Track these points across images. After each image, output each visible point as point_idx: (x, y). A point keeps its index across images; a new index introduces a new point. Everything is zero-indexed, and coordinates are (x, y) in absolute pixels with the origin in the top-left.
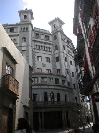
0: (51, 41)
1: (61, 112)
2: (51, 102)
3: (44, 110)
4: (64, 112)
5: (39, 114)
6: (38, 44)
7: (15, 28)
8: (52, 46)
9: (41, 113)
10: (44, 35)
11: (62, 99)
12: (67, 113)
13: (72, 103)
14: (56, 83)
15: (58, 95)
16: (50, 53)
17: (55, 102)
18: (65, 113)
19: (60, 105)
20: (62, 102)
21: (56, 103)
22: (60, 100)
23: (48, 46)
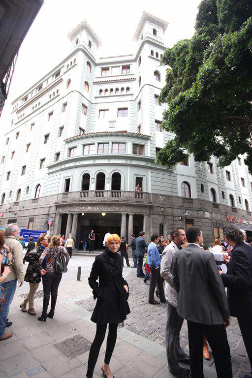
0: (134, 74)
1: (119, 216)
3: (77, 210)
4: (127, 216)
5: (69, 217)
6: (103, 87)
7: (61, 69)
9: (72, 215)
10: (119, 66)
11: (128, 184)
12: (138, 221)
13: (161, 195)
14: (135, 152)
15: (116, 178)
16: (129, 98)
18: (131, 218)
19: (116, 199)
22: (120, 189)
23: (125, 85)
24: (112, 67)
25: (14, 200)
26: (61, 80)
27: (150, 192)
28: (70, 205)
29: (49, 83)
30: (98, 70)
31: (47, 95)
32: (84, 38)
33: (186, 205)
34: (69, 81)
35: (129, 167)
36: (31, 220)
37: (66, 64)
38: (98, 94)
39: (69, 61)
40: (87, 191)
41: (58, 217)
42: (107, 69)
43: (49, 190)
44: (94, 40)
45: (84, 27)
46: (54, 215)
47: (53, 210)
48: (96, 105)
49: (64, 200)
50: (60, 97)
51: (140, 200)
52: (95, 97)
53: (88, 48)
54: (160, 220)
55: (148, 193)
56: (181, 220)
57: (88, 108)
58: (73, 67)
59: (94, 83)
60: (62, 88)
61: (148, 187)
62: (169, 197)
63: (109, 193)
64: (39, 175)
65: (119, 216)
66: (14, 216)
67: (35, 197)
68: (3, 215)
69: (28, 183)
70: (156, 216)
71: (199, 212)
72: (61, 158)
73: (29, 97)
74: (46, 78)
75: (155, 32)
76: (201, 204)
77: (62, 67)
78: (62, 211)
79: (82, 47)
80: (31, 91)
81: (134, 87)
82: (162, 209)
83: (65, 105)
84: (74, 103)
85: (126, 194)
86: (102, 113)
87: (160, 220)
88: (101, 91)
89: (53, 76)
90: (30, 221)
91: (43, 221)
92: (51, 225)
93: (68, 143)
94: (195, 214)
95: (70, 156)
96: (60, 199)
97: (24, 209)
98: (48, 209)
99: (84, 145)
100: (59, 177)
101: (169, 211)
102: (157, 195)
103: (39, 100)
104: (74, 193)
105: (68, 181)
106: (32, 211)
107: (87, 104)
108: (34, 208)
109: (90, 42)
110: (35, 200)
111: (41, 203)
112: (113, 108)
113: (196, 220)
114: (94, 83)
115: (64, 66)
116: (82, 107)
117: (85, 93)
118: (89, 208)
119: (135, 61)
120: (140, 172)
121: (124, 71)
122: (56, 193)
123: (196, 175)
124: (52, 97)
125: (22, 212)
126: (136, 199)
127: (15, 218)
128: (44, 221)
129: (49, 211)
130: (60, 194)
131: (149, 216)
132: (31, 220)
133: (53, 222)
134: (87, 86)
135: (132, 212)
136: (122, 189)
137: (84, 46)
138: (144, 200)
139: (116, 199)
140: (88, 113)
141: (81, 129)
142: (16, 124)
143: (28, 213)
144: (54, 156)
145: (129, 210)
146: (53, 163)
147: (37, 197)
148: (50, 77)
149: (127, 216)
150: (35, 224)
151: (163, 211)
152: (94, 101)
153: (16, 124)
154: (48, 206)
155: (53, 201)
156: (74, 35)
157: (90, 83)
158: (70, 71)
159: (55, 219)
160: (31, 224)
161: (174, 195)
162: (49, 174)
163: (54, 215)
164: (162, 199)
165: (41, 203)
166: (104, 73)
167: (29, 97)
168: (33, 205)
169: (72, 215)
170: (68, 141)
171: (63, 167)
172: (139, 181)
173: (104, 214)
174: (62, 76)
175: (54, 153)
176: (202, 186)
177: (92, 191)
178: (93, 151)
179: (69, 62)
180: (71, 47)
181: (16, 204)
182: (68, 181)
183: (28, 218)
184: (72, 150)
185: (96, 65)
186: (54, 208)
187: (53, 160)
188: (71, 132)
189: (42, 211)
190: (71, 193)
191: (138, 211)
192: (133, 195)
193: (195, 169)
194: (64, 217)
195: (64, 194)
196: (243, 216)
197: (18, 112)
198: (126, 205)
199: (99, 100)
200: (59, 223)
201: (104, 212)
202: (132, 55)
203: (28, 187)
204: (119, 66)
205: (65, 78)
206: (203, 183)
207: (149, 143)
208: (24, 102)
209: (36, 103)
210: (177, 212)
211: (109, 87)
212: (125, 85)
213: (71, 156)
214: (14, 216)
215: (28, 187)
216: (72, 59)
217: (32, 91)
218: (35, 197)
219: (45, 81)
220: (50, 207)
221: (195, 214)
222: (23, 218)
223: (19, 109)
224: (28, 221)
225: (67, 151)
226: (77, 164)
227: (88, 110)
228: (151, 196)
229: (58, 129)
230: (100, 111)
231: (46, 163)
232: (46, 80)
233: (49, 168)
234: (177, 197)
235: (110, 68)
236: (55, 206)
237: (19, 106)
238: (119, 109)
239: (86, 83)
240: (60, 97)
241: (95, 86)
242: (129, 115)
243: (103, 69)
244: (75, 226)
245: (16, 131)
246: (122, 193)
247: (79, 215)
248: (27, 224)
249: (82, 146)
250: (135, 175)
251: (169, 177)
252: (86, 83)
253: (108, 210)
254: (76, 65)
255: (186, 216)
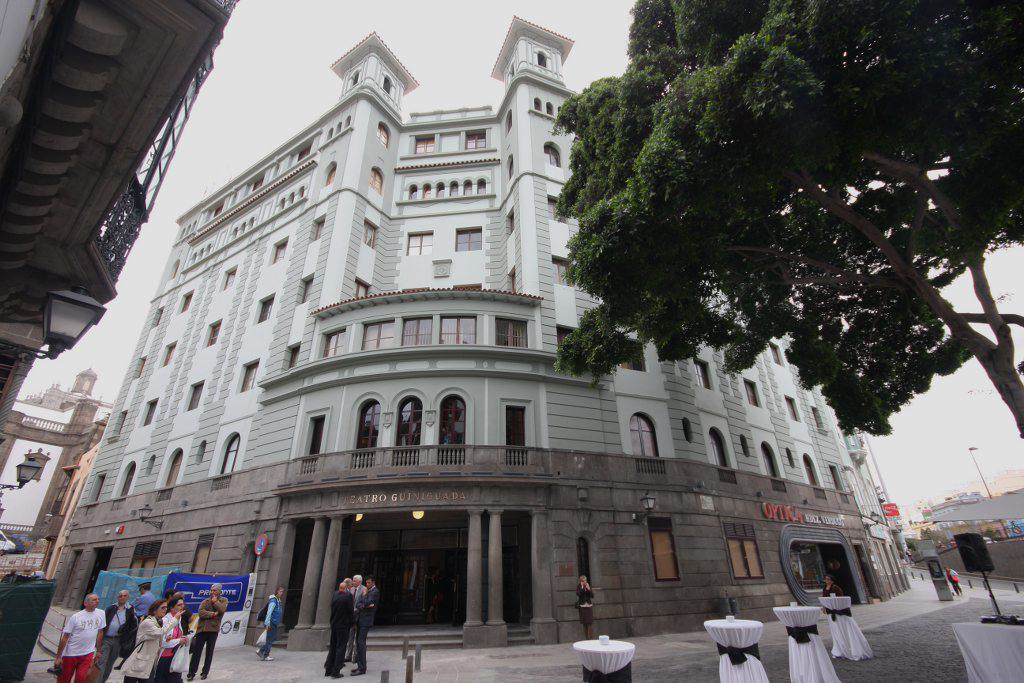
0: (495, 151)
1: (460, 520)
2: (389, 454)
3: (340, 506)
4: (485, 517)
5: (317, 528)
6: (420, 180)
8: (498, 170)
9: (327, 522)
11: (484, 427)
12: (517, 527)
13: (577, 453)
14: (501, 340)
15: (452, 409)
16: (484, 205)
17: (423, 454)
18: (495, 523)
19: (452, 468)
20: (475, 448)
21: (427, 460)
23: (474, 175)
24: (442, 135)
25: (160, 484)
26: (313, 165)
27: (545, 445)
28: (321, 493)
29: (282, 170)
30: (405, 144)
31: (276, 199)
32: (372, 71)
33: (647, 478)
34: (333, 168)
35: (486, 381)
36: (206, 541)
37: (326, 129)
38: (406, 198)
39: (336, 123)
40: (371, 449)
41: (284, 528)
42: (430, 139)
43: (264, 450)
44: (398, 76)
45: (373, 47)
46: (272, 526)
47: (270, 510)
48: (401, 221)
49: (306, 477)
50: (307, 205)
51: (520, 469)
52: (398, 204)
53: (381, 92)
54: (577, 525)
55: (541, 450)
56: (637, 521)
57: (381, 230)
58: (342, 135)
59: (398, 171)
60: (314, 185)
61: (540, 432)
62: (599, 457)
63: (433, 453)
64: (241, 408)
65: (460, 520)
66: (154, 530)
67: (222, 472)
68: (121, 532)
69: (203, 432)
70: (565, 515)
71: (684, 496)
72: (301, 362)
73: (228, 206)
74: (275, 161)
75: (542, 60)
76: (687, 473)
77: (315, 136)
78: (297, 510)
79: (367, 91)
80: (233, 190)
81: (497, 179)
82: (583, 494)
83: (320, 223)
84: (344, 217)
85: (482, 453)
86: (415, 241)
87: (577, 525)
88: (414, 189)
89: (292, 155)
90: (199, 546)
91: (239, 543)
92: (263, 556)
93: (323, 318)
94: (672, 501)
95: (326, 353)
96: (295, 474)
97: (188, 508)
98: (256, 507)
99: (366, 325)
100: (291, 412)
101: (599, 496)
102: (562, 455)
103: (255, 213)
104: (334, 458)
105: (318, 423)
106: (210, 513)
107: (376, 219)
108: (216, 504)
109: (387, 81)
110: (222, 481)
111: (236, 490)
112: (445, 230)
113: (677, 519)
114: (398, 171)
115: (320, 133)
116: (363, 229)
117: (373, 195)
118: (374, 498)
119: (497, 120)
120: (515, 393)
121: (472, 144)
122: (286, 459)
123: (666, 396)
124: (287, 206)
125: (179, 517)
126: (506, 468)
127: (158, 538)
128: (242, 543)
129: (258, 512)
130: (295, 460)
131: (546, 515)
132: (206, 541)
133: (268, 544)
134: (378, 178)
135: (498, 505)
136: (469, 440)
137: (372, 90)
138: (530, 470)
139: (452, 468)
140: (379, 242)
141: (359, 282)
142: (185, 273)
143: (196, 522)
144: (282, 355)
145: (488, 499)
146: (279, 374)
147: (228, 470)
148: (287, 155)
149: (485, 517)
150: (216, 553)
151: (583, 500)
152: (394, 213)
153: (185, 273)
154: (258, 497)
155: (273, 482)
156: (347, 65)
157: (387, 171)
158: (336, 143)
159: (275, 537)
160: (204, 553)
161: (611, 450)
162: (266, 404)
163: (272, 526)
164: (579, 464)
165: (236, 490)
166: (421, 149)
167: (228, 206)
168: (215, 497)
169: (327, 522)
170: (322, 315)
171: (307, 384)
172: (515, 418)
173: (418, 515)
174: (315, 154)
175: (284, 348)
176: (686, 424)
177: (384, 450)
178: (390, 339)
179: (334, 124)
180: (335, 90)
181: (165, 493)
182: (318, 423)
183: (195, 536)
184: (334, 338)
185: (402, 129)
186: (275, 502)
187: (280, 365)
188: (330, 292)
189: (240, 514)
190: (325, 455)
191: (513, 502)
192: (499, 457)
193: (664, 378)
194: (302, 530)
195: (305, 460)
196: (805, 502)
197: (195, 241)
198: (480, 486)
199: (408, 211)
200: (286, 546)
201: (418, 508)
202: (489, 108)
203: (204, 444)
204: (458, 133)
205: (322, 160)
206: (684, 415)
207: (537, 314)
208: (212, 218)
209: (246, 218)
210: (624, 498)
211: (434, 179)
212: (474, 175)
213: (331, 353)
214: (154, 530)
215: (204, 444)
216: (342, 118)
217: (237, 190)
218: (222, 472)
219: (271, 166)
220: (262, 501)
221: (672, 501)
222: (181, 537)
223: (198, 234)
224: (193, 545)
225: (317, 340)
226: (346, 374)
227: (379, 235)
228: (550, 458)
229: (298, 283)
230: (411, 235)
231: (261, 374)
232: (274, 164)
233: (268, 387)
234: (622, 457)
235: (437, 137)
236: (278, 495)
237: (199, 226)
238: (460, 232)
239: (377, 171)
240: (307, 205)
241: (399, 179)
242: (486, 246)
243: (419, 140)
244: (333, 555)
245: (185, 290)
246: (469, 452)
247: (348, 520)
248: (190, 557)
249: (361, 327)
250: (502, 400)
251: (596, 404)
252: (377, 171)
253: (431, 503)
254: (352, 130)
255: (649, 509)
